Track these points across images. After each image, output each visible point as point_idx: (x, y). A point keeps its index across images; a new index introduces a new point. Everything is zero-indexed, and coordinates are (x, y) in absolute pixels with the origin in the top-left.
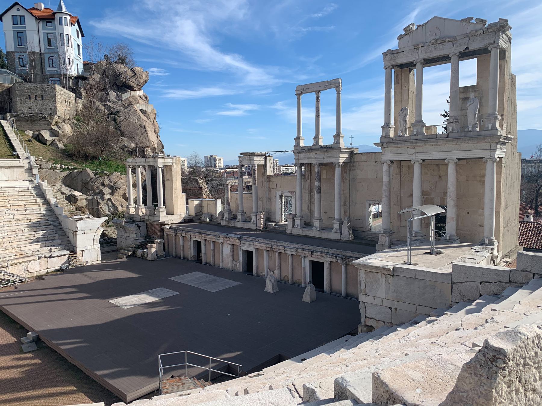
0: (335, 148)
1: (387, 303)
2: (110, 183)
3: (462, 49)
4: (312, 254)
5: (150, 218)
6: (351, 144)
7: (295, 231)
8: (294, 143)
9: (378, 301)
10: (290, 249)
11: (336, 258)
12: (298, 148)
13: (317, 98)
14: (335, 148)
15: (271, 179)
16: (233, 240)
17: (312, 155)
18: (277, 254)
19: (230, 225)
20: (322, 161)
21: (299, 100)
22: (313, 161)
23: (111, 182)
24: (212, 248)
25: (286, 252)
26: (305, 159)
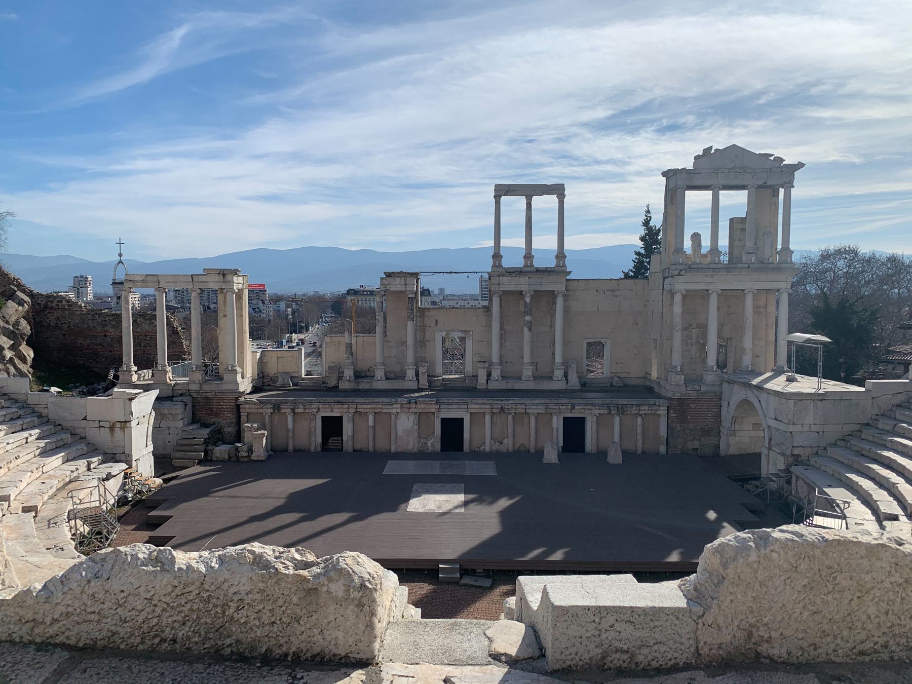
0: (559, 270)
1: (814, 428)
2: (6, 326)
3: (761, 182)
4: (573, 408)
5: (206, 387)
6: (120, 255)
7: (493, 385)
8: (491, 262)
9: (806, 428)
10: (536, 407)
11: (609, 408)
12: (500, 269)
13: (529, 205)
14: (559, 270)
15: (426, 313)
16: (422, 406)
17: (523, 280)
18: (510, 417)
19: (361, 387)
20: (539, 288)
21: (498, 203)
22: (523, 288)
23: (7, 322)
24: (371, 423)
25: (528, 411)
26: (509, 284)
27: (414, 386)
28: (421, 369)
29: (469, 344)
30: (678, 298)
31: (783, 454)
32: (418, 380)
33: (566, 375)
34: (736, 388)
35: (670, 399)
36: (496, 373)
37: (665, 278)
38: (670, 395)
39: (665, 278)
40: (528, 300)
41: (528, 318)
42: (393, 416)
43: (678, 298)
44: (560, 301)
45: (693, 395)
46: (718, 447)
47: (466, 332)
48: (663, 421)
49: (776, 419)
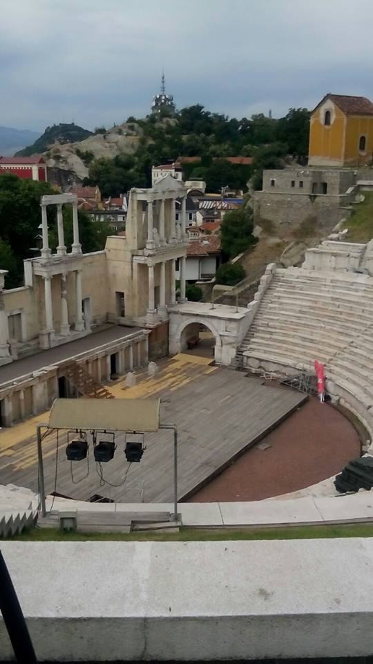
27: (10, 361)
28: (13, 346)
29: (23, 317)
30: (151, 270)
31: (234, 347)
32: (11, 354)
33: (85, 326)
34: (184, 317)
35: (150, 329)
36: (52, 336)
37: (133, 256)
38: (152, 326)
39: (133, 256)
40: (64, 279)
41: (65, 292)
42: (34, 388)
43: (151, 270)
44: (79, 276)
45: (160, 323)
46: (168, 349)
47: (21, 309)
48: (147, 342)
49: (226, 331)
